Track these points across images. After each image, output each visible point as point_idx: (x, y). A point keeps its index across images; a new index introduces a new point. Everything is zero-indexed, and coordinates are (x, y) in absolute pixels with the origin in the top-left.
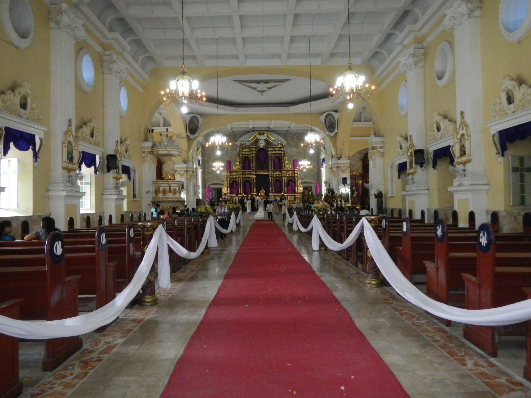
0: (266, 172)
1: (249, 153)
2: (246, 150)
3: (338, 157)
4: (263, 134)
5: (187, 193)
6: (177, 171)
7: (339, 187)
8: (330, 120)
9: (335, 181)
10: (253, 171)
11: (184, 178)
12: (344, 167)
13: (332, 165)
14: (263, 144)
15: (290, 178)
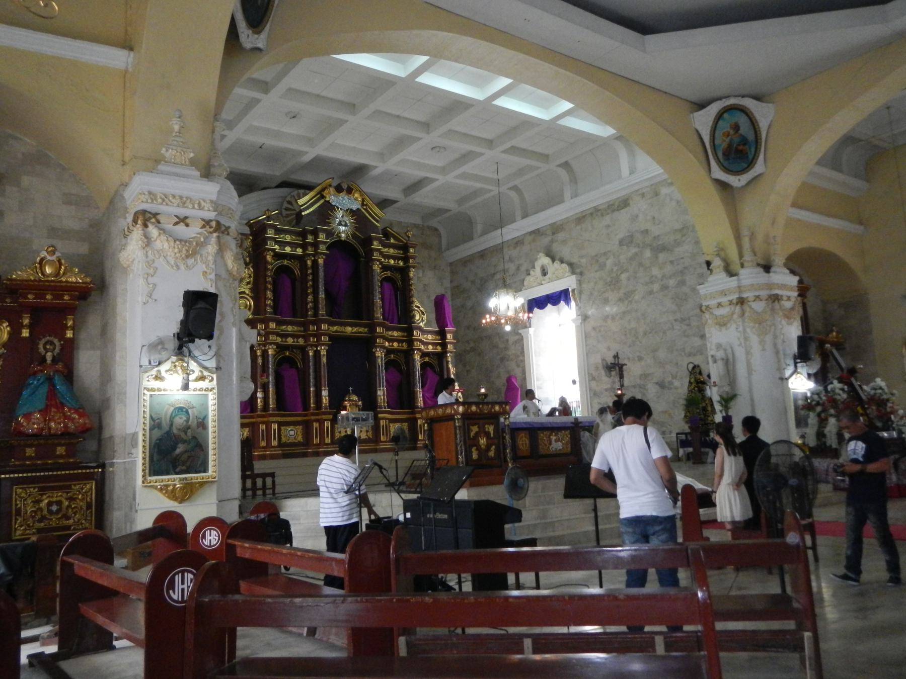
0: (361, 330)
1: (299, 251)
2: (288, 238)
3: (758, 265)
4: (350, 191)
5: (218, 368)
6: (155, 215)
7: (781, 370)
8: (736, 128)
9: (764, 350)
10: (317, 323)
11: (201, 267)
12: (789, 298)
13: (740, 288)
14: (346, 225)
15: (427, 359)
